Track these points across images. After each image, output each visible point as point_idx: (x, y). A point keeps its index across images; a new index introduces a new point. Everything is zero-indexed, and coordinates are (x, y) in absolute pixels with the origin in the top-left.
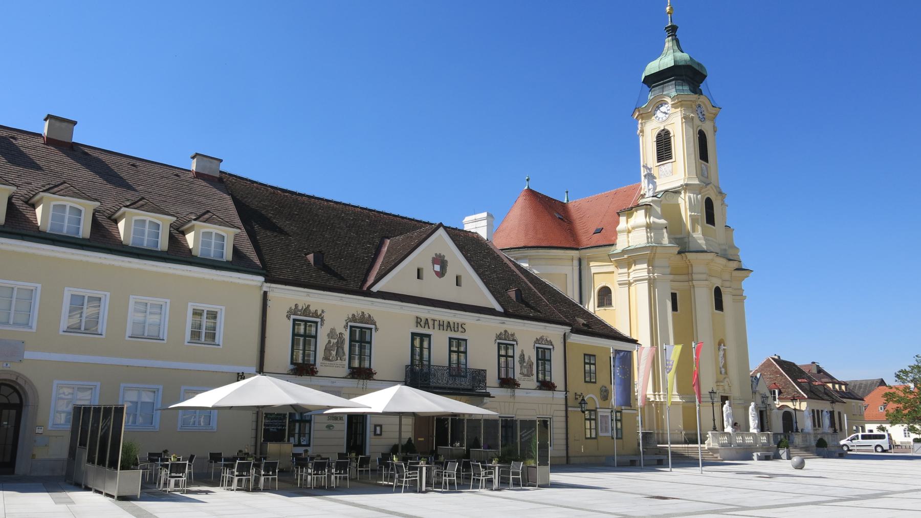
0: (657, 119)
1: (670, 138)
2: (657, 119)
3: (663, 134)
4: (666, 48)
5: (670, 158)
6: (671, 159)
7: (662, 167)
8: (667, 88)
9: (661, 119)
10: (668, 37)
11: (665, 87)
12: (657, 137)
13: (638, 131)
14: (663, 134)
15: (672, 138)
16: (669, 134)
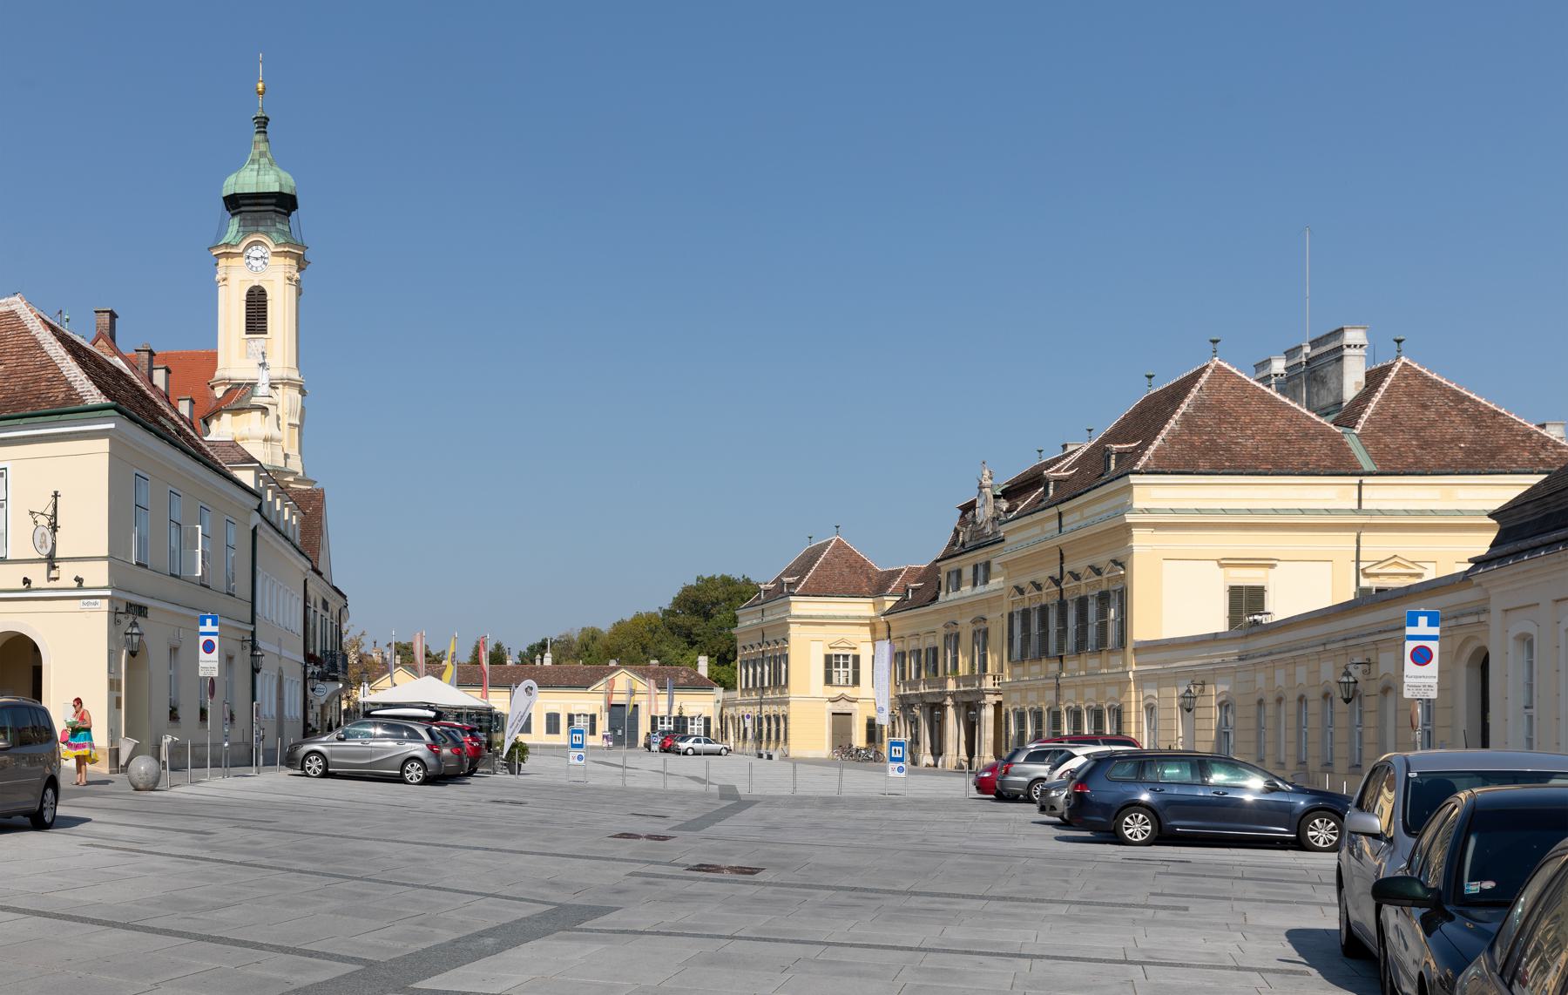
0: (250, 266)
1: (266, 301)
2: (250, 266)
3: (256, 292)
4: (254, 152)
5: (264, 330)
6: (266, 333)
7: (252, 342)
8: (263, 223)
9: (254, 269)
10: (258, 132)
11: (261, 219)
12: (248, 295)
13: (218, 277)
14: (256, 292)
15: (269, 303)
16: (265, 295)
